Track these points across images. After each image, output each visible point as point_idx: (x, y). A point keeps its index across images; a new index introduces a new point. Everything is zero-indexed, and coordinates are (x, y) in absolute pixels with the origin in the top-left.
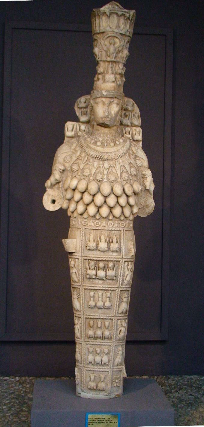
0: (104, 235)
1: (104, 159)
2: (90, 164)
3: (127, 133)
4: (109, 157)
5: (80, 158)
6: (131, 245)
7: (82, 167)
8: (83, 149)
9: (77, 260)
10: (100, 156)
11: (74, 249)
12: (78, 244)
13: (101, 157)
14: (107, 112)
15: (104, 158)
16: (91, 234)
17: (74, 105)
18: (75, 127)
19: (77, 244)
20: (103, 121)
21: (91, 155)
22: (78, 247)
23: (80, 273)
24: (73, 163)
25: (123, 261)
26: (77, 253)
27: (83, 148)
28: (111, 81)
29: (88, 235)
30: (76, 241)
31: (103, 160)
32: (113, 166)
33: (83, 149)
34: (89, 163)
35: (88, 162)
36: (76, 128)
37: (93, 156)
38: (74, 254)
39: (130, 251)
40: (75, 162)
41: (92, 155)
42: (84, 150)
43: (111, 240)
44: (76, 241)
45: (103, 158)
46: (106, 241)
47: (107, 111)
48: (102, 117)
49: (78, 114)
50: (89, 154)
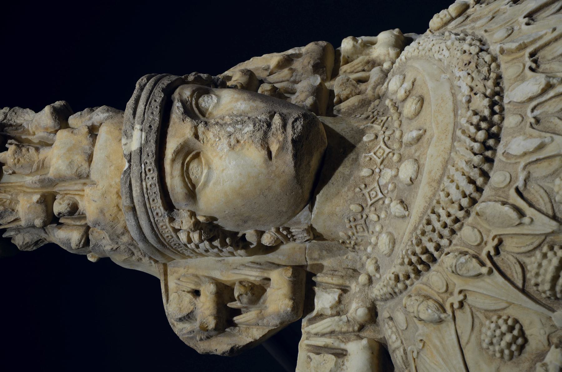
1: (493, 113)
2: (522, 177)
3: (362, 86)
4: (480, 88)
5: (490, 247)
7: (546, 219)
8: (438, 248)
10: (472, 130)
13: (478, 128)
14: (239, 126)
15: (487, 112)
17: (209, 357)
18: (320, 342)
20: (282, 148)
21: (469, 189)
24: (523, 291)
27: (431, 247)
28: (85, 142)
31: (496, 118)
32: (532, 55)
33: (438, 248)
34: (520, 183)
35: (512, 192)
36: (332, 333)
37: (475, 174)
40: (520, 284)
41: (471, 181)
42: (444, 242)
45: (484, 119)
47: (230, 129)
48: (264, 153)
49: (257, 334)
50: (465, 202)
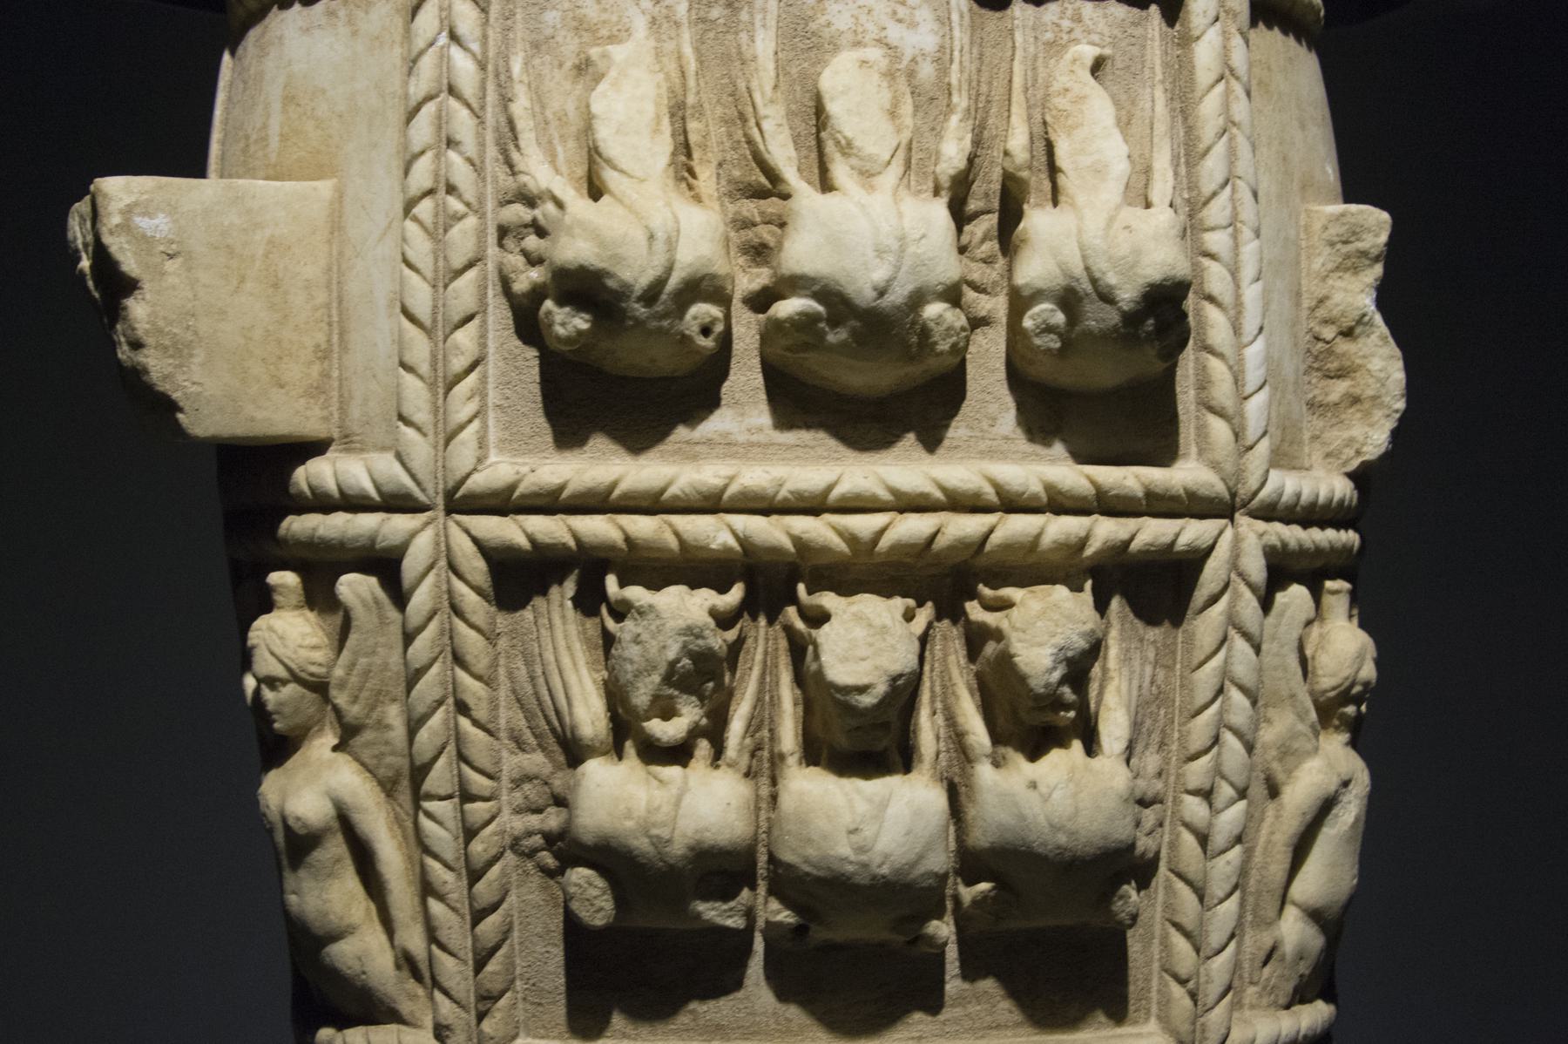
0: (874, 53)
6: (1351, 264)
9: (355, 587)
11: (297, 372)
12: (374, 278)
16: (618, 52)
19: (353, 287)
22: (378, 333)
23: (441, 836)
25: (1256, 567)
26: (349, 442)
29: (563, 96)
30: (336, 224)
38: (318, 473)
39: (1340, 388)
43: (1018, 141)
44: (336, 224)
46: (912, 159)
